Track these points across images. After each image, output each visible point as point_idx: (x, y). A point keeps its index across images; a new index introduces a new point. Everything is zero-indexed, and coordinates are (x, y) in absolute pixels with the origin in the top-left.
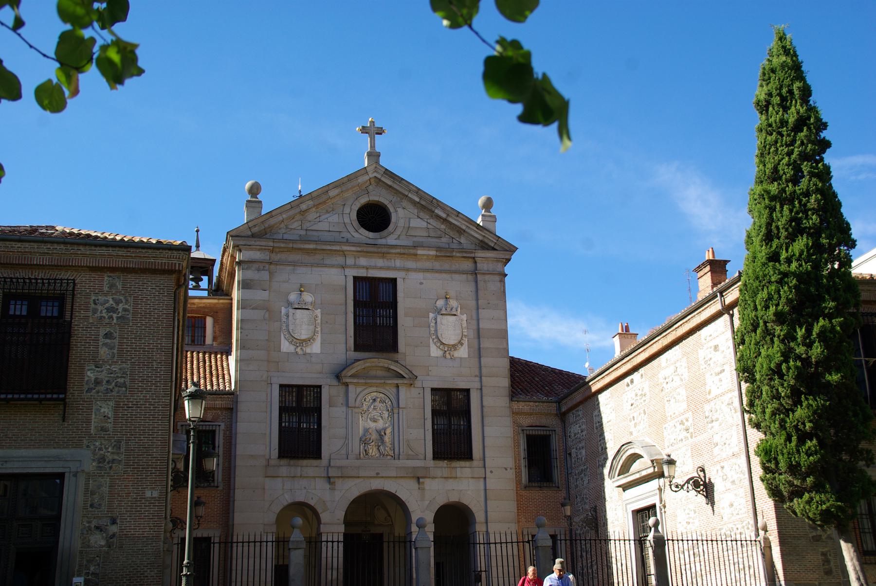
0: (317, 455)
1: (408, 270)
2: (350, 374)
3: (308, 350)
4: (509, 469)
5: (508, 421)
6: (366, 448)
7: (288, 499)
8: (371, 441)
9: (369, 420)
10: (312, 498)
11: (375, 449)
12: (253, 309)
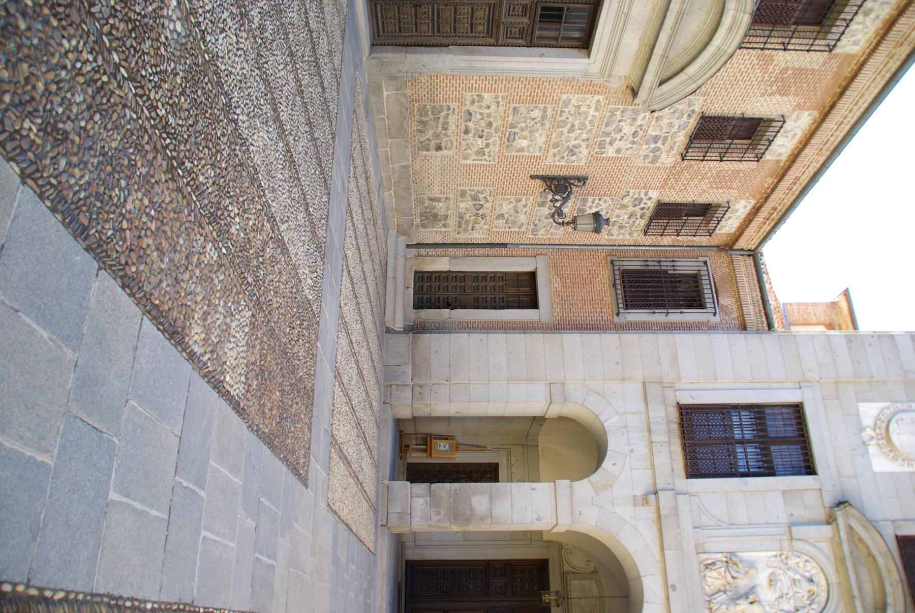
0: (694, 471)
2: (854, 524)
3: (873, 449)
6: (719, 564)
8: (735, 574)
9: (770, 571)
10: (614, 464)
11: (719, 583)
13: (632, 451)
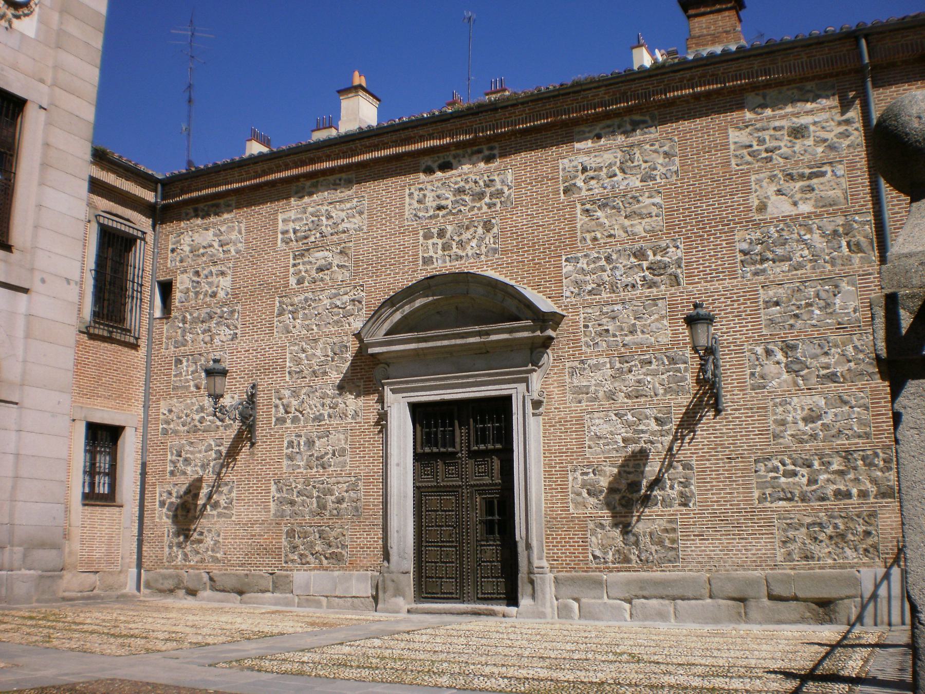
4: (73, 284)
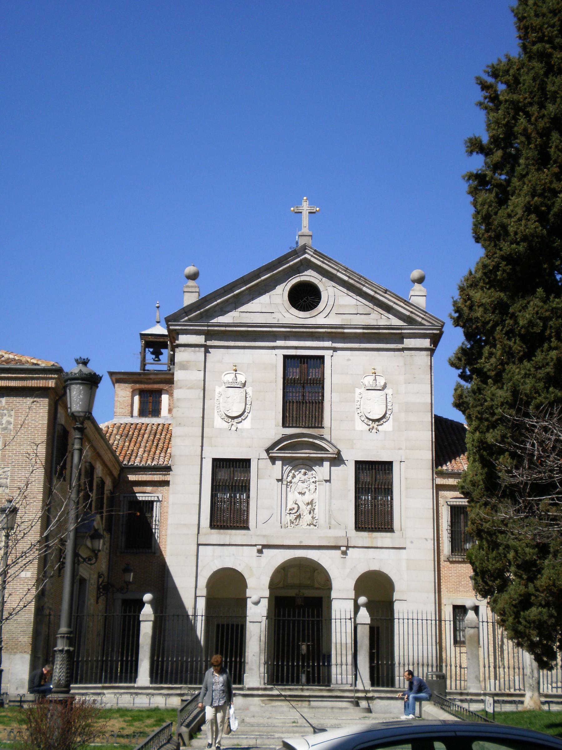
1: (335, 349)
5: (429, 493)
7: (217, 565)
10: (240, 565)
12: (189, 388)
13: (233, 555)
